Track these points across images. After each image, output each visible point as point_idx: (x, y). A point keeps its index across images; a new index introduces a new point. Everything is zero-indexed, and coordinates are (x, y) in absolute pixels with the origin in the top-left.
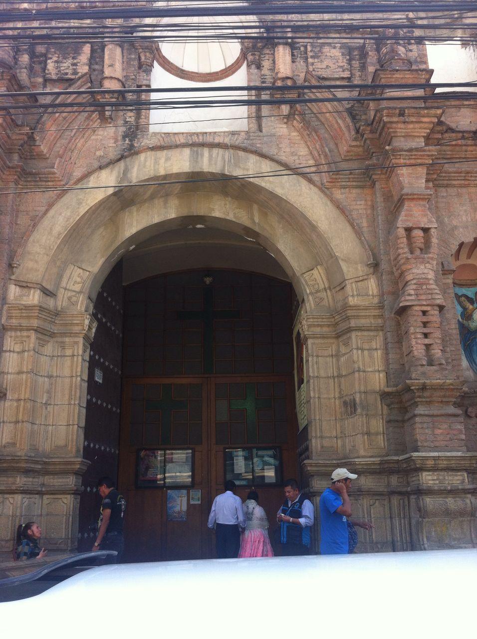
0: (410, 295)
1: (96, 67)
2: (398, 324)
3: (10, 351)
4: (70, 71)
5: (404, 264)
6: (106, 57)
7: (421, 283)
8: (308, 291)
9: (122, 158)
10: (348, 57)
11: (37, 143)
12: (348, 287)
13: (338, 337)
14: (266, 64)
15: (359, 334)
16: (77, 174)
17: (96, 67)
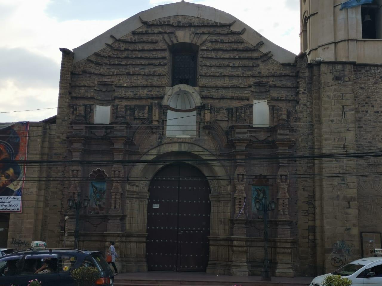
0: (236, 194)
1: (150, 114)
2: (235, 200)
3: (128, 204)
4: (142, 116)
5: (236, 184)
6: (153, 112)
7: (240, 191)
8: (212, 187)
9: (158, 146)
10: (228, 113)
11: (134, 141)
12: (222, 188)
13: (219, 201)
14: (202, 115)
15: (224, 202)
16: (145, 150)
17: (150, 114)
